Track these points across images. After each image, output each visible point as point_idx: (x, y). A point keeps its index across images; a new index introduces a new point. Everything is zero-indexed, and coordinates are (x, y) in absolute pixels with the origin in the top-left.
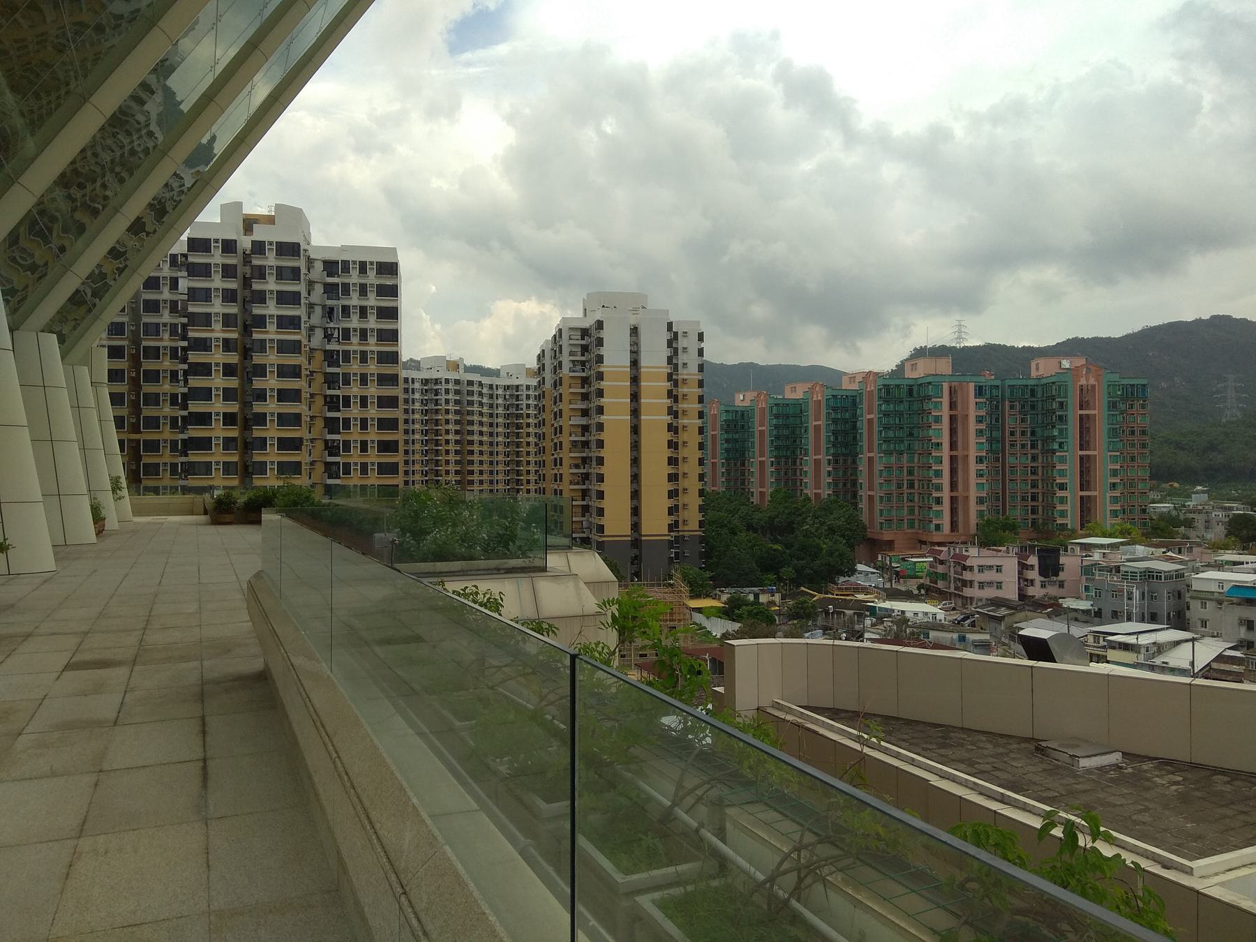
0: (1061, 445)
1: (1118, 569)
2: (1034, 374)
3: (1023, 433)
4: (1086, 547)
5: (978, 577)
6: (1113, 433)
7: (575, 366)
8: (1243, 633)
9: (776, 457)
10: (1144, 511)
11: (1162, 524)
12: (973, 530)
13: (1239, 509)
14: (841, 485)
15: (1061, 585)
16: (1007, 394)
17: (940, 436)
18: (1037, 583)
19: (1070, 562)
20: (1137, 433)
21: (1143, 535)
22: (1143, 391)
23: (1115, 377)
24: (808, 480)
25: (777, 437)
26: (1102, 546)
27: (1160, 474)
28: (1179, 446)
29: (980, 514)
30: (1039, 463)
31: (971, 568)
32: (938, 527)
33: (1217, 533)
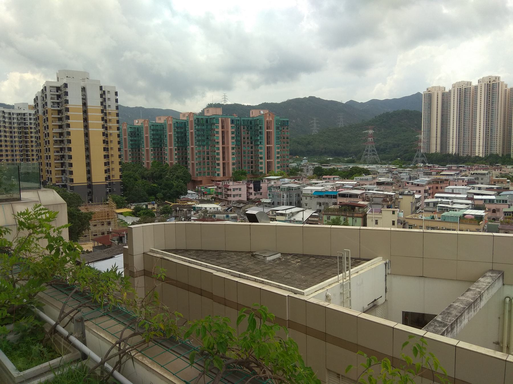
0: (260, 142)
1: (279, 187)
2: (251, 116)
3: (248, 138)
4: (269, 180)
5: (233, 193)
6: (278, 138)
8: (318, 207)
9: (153, 148)
10: (288, 166)
11: (293, 171)
13: (317, 165)
15: (261, 194)
16: (242, 123)
18: (253, 194)
19: (264, 185)
20: (285, 138)
21: (288, 175)
22: (288, 123)
23: (278, 118)
25: (154, 139)
26: (274, 179)
27: (293, 153)
28: (299, 143)
29: (233, 169)
31: (230, 190)
32: (218, 175)
33: (310, 173)
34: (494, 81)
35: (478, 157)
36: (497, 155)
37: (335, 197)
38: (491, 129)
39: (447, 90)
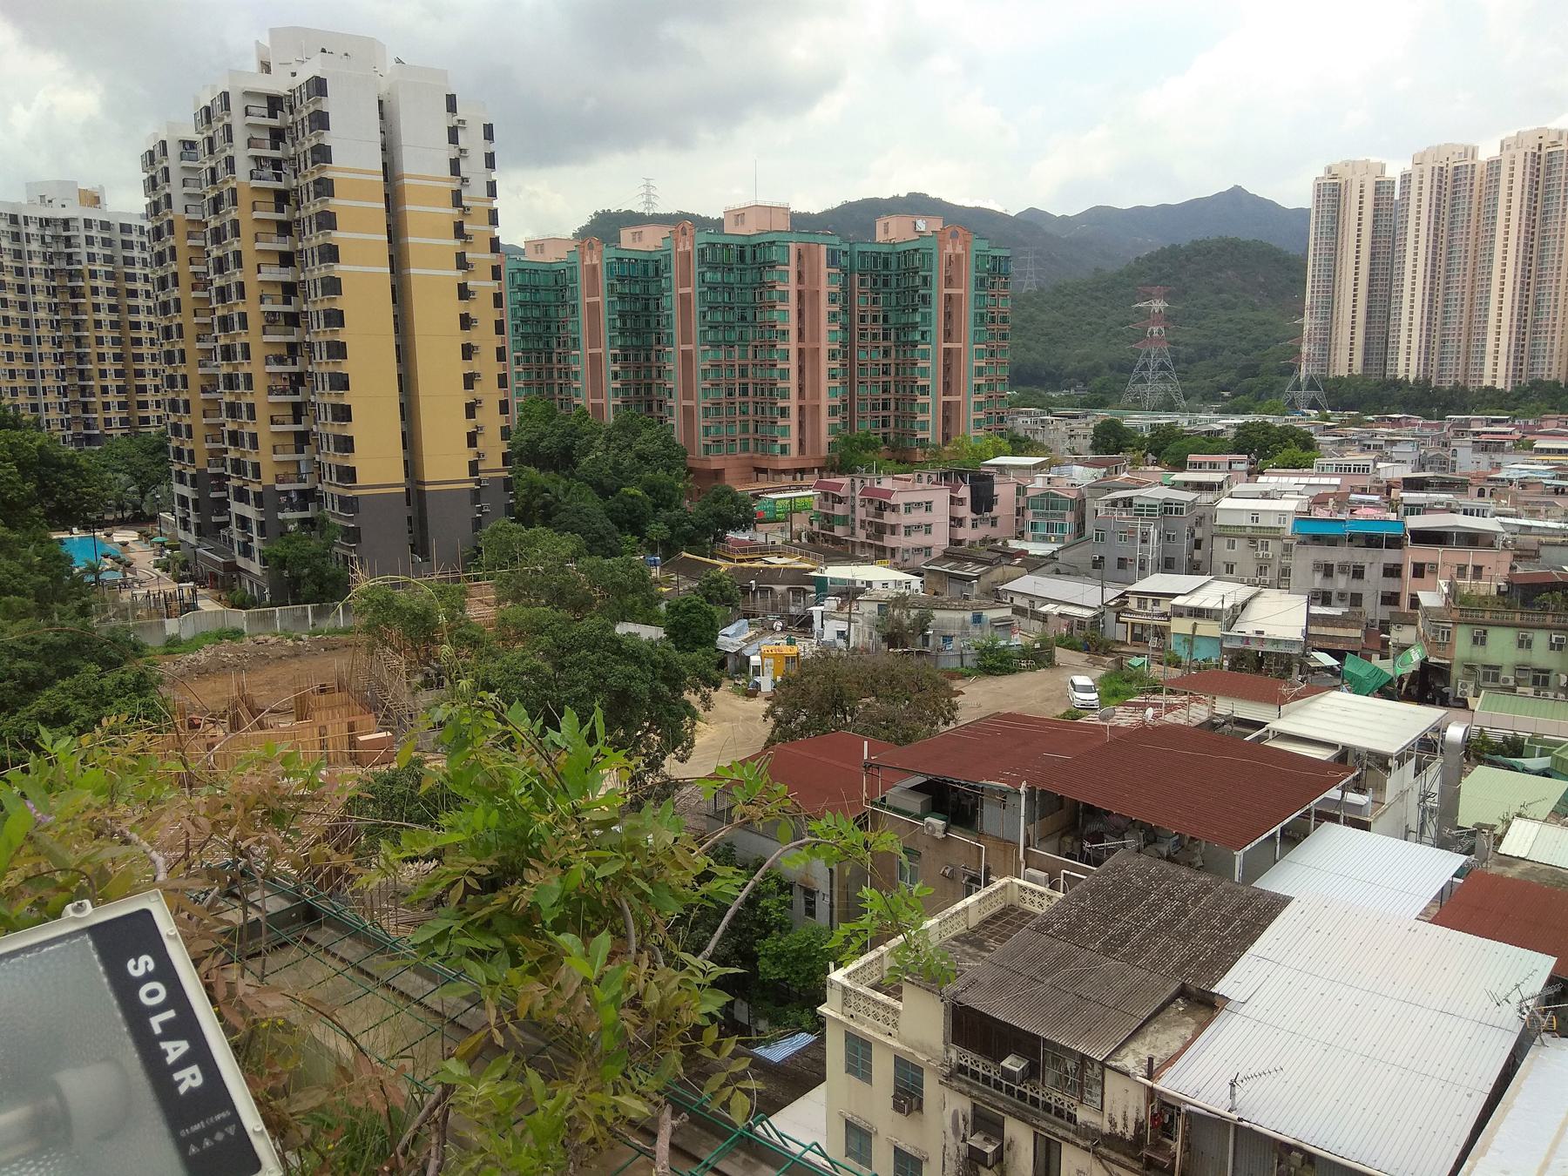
0: (923, 333)
3: (875, 319)
5: (905, 519)
7: (260, 167)
8: (1318, 582)
9: (524, 351)
12: (824, 452)
14: (632, 393)
16: (857, 265)
17: (786, 322)
23: (984, 245)
24: (582, 384)
25: (525, 321)
29: (833, 429)
30: (891, 360)
31: (894, 508)
32: (784, 449)
34: (1554, 144)
35: (1491, 389)
36: (1557, 383)
37: (1395, 543)
38: (1537, 302)
39: (1394, 172)
